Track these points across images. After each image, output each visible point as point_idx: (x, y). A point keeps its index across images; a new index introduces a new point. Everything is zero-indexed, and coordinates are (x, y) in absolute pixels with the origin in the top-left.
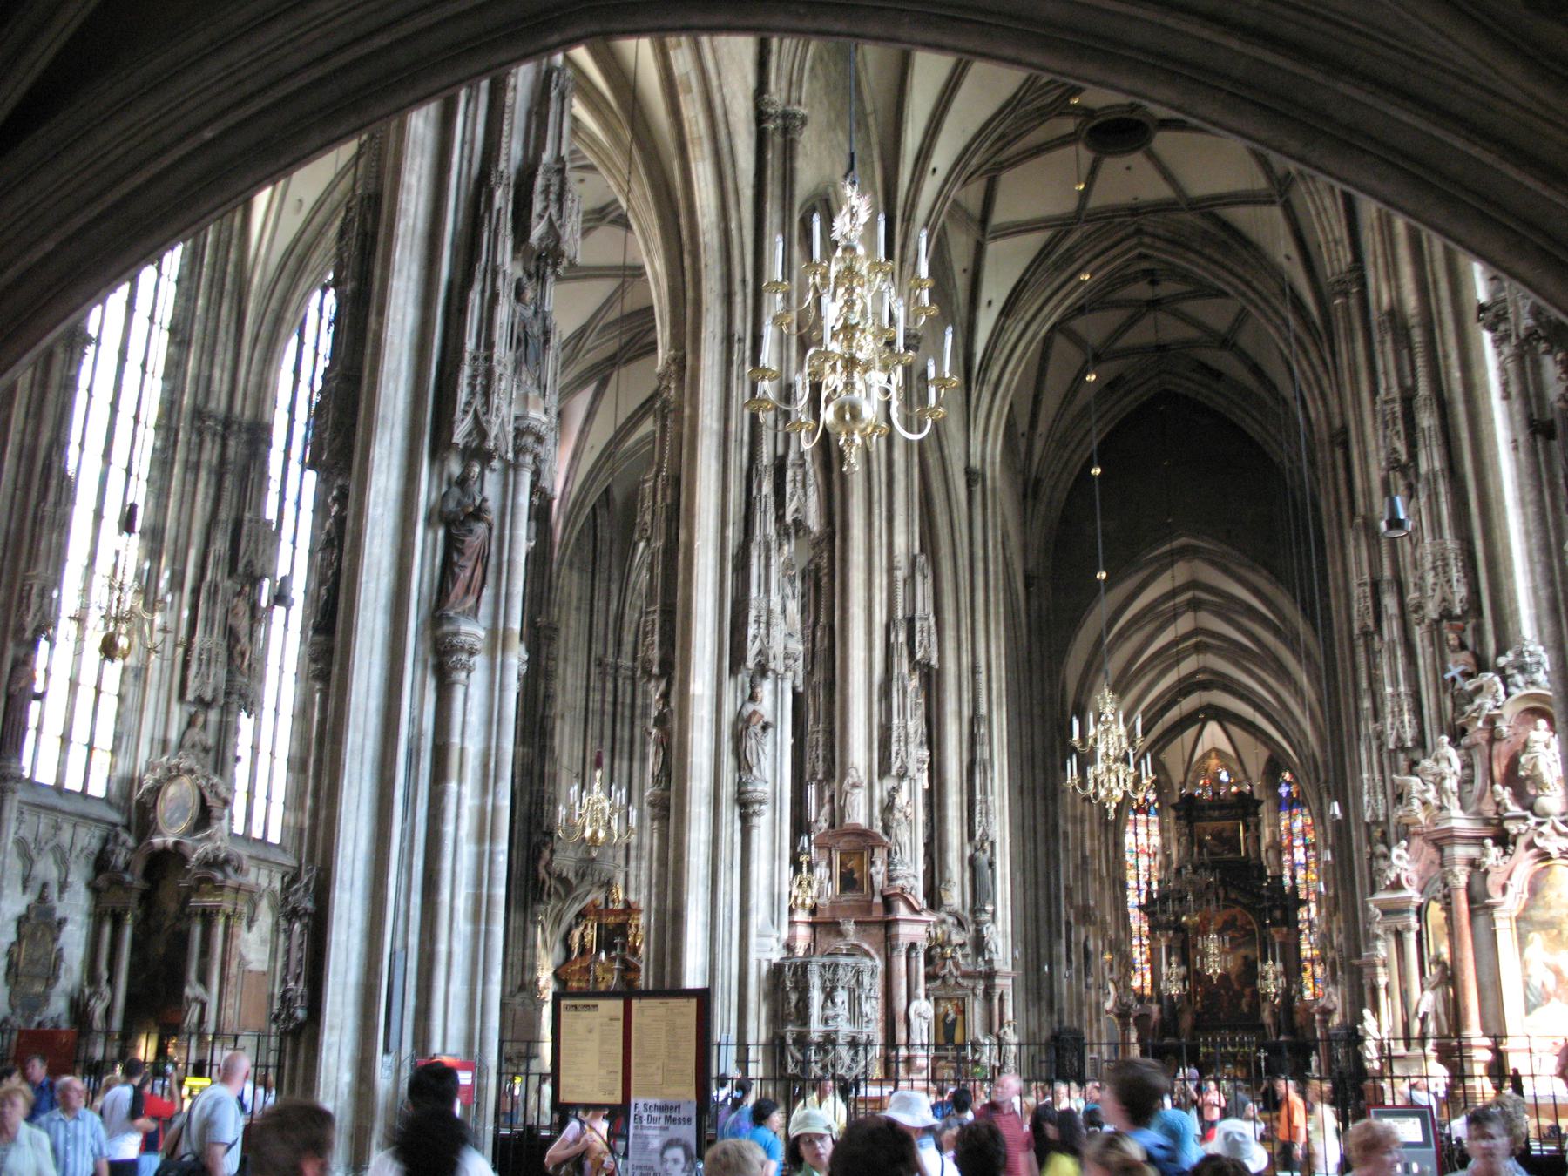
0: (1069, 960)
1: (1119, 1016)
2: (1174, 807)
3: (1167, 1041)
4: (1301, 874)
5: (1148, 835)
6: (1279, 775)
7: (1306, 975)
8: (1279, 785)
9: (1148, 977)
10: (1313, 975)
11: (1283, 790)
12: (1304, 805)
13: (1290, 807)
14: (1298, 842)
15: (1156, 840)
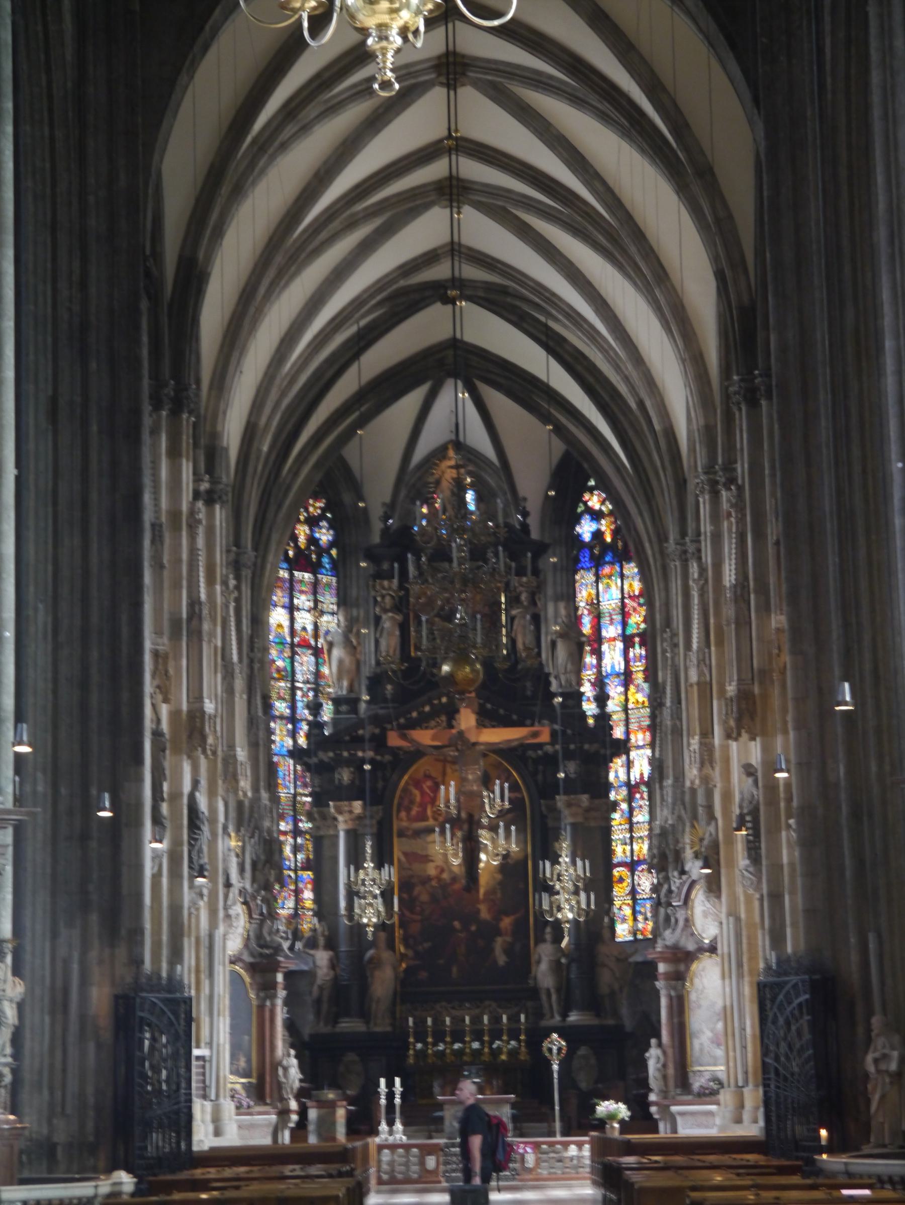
0: (157, 820)
1: (252, 968)
2: (370, 555)
3: (349, 1025)
4: (615, 691)
5: (317, 609)
6: (579, 499)
7: (620, 892)
8: (577, 520)
9: (308, 895)
10: (633, 893)
11: (586, 529)
12: (622, 557)
13: (597, 563)
14: (610, 631)
15: (329, 622)
